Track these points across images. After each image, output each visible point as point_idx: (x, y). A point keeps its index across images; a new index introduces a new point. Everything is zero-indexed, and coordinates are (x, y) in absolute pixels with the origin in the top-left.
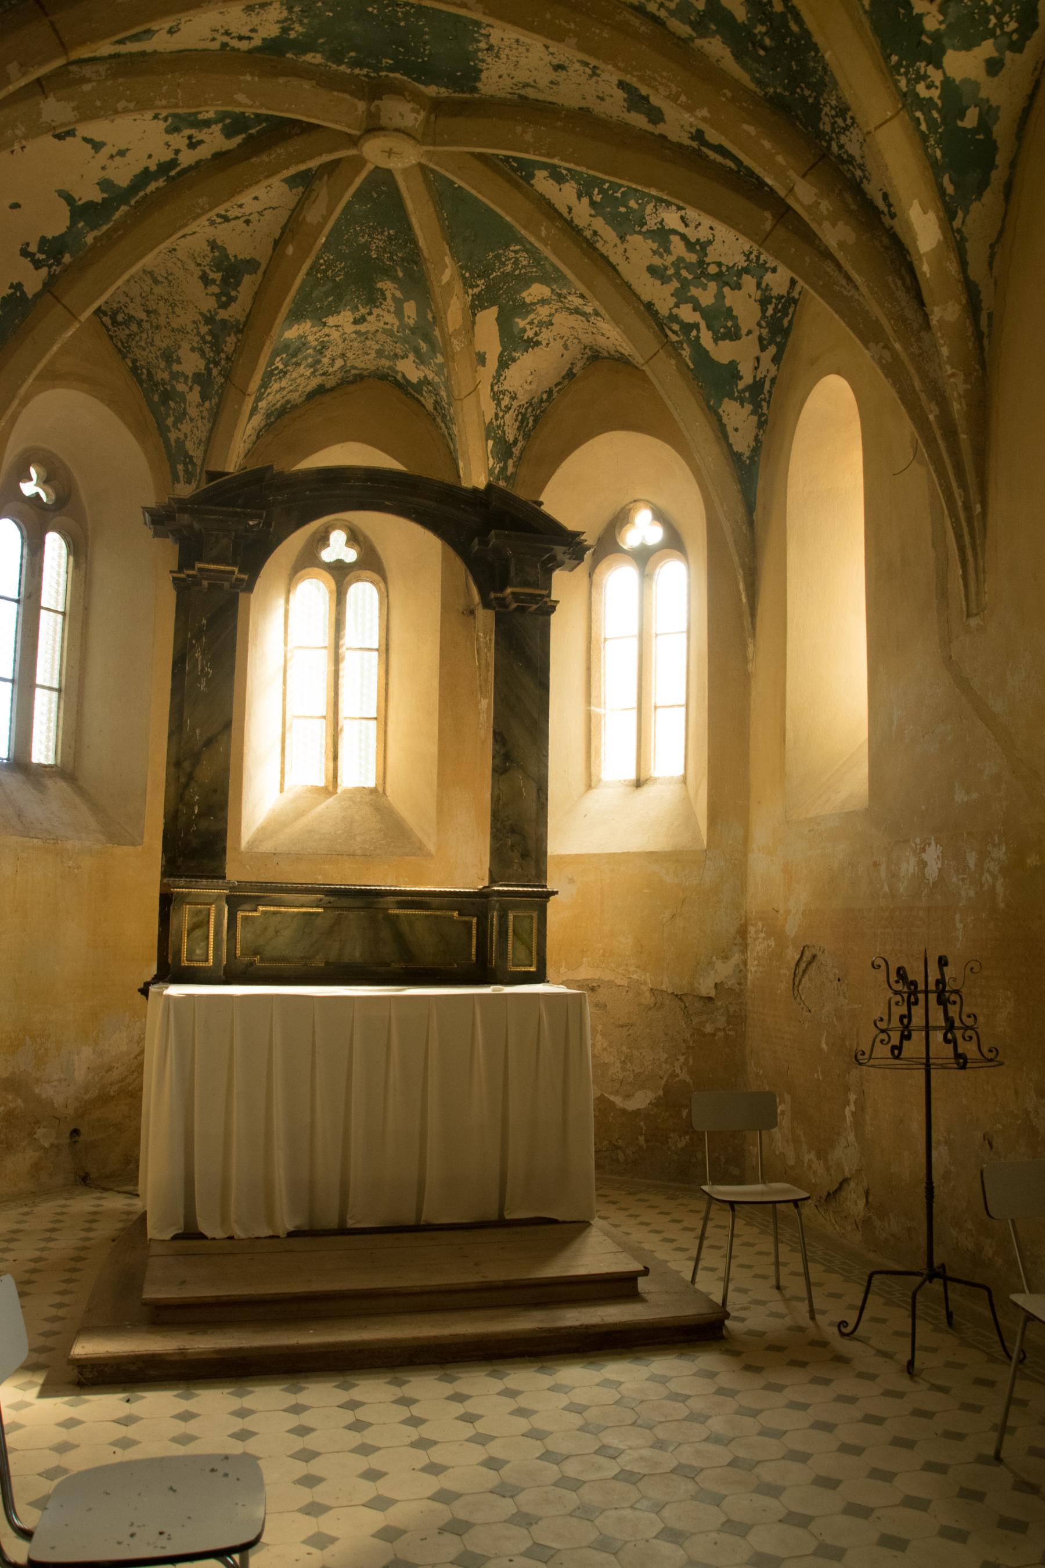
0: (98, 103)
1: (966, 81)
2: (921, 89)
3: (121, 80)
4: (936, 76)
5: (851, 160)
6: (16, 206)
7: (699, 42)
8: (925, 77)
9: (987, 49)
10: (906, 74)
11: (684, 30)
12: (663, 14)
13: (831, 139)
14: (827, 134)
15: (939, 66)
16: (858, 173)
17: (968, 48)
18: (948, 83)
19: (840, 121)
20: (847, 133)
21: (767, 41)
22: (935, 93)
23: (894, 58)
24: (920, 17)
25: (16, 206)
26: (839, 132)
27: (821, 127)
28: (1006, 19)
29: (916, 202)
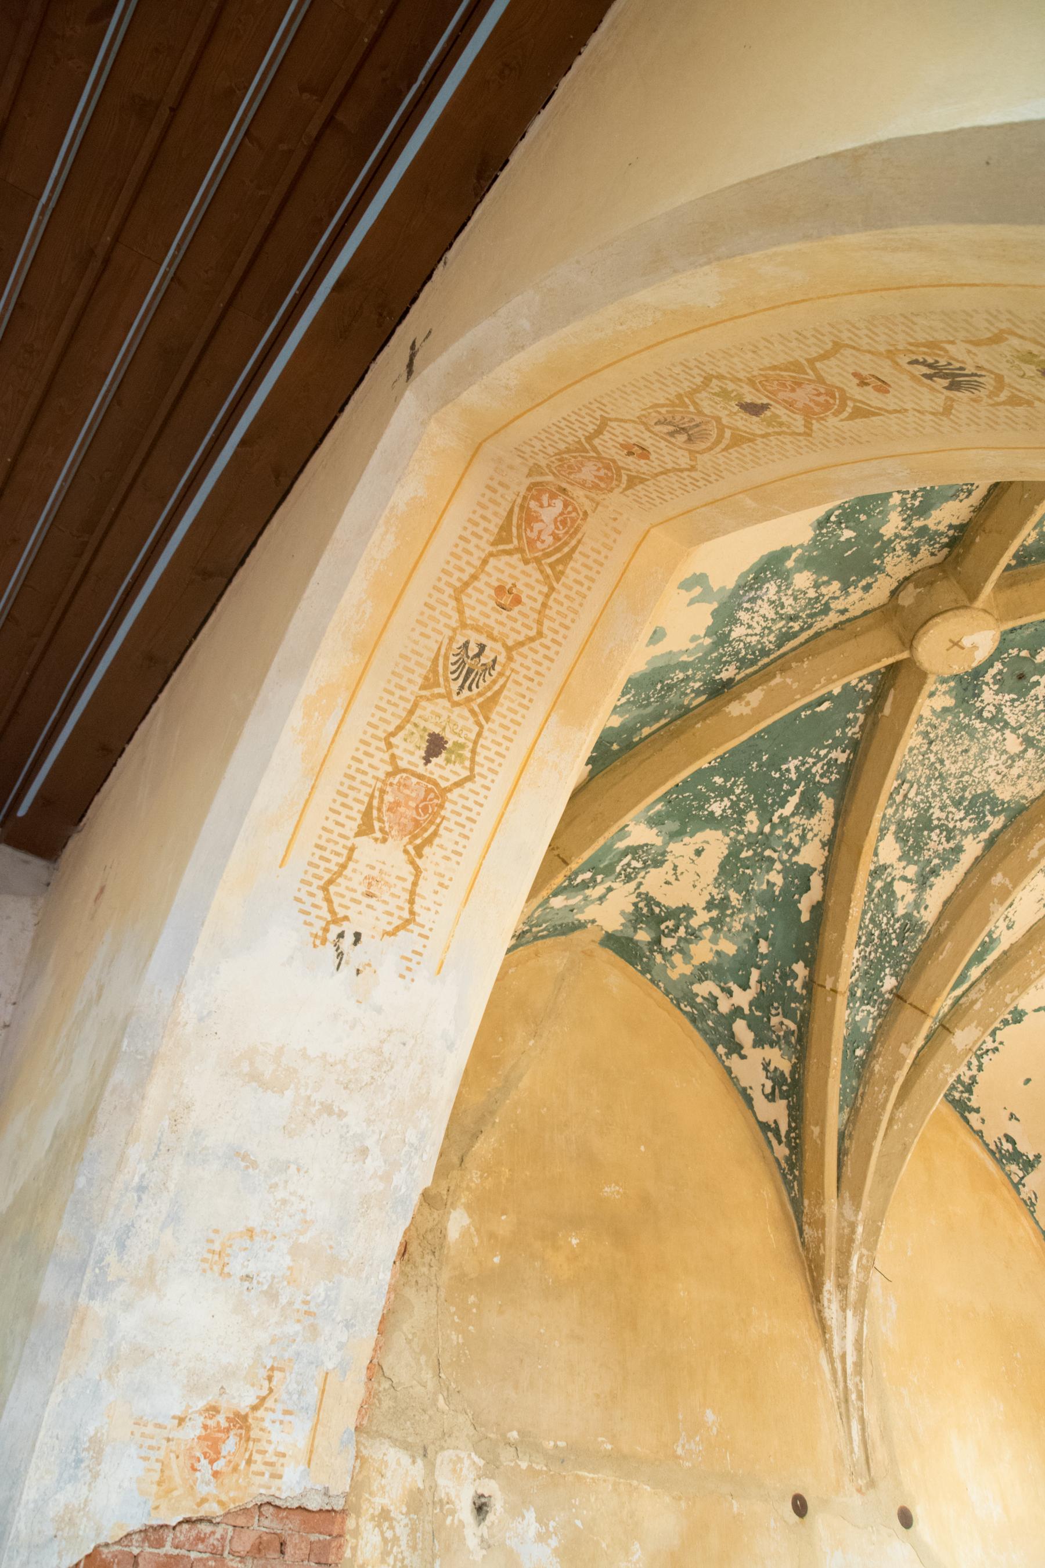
0: (992, 1010)
3: (998, 983)
6: (1028, 1081)
25: (1028, 1081)
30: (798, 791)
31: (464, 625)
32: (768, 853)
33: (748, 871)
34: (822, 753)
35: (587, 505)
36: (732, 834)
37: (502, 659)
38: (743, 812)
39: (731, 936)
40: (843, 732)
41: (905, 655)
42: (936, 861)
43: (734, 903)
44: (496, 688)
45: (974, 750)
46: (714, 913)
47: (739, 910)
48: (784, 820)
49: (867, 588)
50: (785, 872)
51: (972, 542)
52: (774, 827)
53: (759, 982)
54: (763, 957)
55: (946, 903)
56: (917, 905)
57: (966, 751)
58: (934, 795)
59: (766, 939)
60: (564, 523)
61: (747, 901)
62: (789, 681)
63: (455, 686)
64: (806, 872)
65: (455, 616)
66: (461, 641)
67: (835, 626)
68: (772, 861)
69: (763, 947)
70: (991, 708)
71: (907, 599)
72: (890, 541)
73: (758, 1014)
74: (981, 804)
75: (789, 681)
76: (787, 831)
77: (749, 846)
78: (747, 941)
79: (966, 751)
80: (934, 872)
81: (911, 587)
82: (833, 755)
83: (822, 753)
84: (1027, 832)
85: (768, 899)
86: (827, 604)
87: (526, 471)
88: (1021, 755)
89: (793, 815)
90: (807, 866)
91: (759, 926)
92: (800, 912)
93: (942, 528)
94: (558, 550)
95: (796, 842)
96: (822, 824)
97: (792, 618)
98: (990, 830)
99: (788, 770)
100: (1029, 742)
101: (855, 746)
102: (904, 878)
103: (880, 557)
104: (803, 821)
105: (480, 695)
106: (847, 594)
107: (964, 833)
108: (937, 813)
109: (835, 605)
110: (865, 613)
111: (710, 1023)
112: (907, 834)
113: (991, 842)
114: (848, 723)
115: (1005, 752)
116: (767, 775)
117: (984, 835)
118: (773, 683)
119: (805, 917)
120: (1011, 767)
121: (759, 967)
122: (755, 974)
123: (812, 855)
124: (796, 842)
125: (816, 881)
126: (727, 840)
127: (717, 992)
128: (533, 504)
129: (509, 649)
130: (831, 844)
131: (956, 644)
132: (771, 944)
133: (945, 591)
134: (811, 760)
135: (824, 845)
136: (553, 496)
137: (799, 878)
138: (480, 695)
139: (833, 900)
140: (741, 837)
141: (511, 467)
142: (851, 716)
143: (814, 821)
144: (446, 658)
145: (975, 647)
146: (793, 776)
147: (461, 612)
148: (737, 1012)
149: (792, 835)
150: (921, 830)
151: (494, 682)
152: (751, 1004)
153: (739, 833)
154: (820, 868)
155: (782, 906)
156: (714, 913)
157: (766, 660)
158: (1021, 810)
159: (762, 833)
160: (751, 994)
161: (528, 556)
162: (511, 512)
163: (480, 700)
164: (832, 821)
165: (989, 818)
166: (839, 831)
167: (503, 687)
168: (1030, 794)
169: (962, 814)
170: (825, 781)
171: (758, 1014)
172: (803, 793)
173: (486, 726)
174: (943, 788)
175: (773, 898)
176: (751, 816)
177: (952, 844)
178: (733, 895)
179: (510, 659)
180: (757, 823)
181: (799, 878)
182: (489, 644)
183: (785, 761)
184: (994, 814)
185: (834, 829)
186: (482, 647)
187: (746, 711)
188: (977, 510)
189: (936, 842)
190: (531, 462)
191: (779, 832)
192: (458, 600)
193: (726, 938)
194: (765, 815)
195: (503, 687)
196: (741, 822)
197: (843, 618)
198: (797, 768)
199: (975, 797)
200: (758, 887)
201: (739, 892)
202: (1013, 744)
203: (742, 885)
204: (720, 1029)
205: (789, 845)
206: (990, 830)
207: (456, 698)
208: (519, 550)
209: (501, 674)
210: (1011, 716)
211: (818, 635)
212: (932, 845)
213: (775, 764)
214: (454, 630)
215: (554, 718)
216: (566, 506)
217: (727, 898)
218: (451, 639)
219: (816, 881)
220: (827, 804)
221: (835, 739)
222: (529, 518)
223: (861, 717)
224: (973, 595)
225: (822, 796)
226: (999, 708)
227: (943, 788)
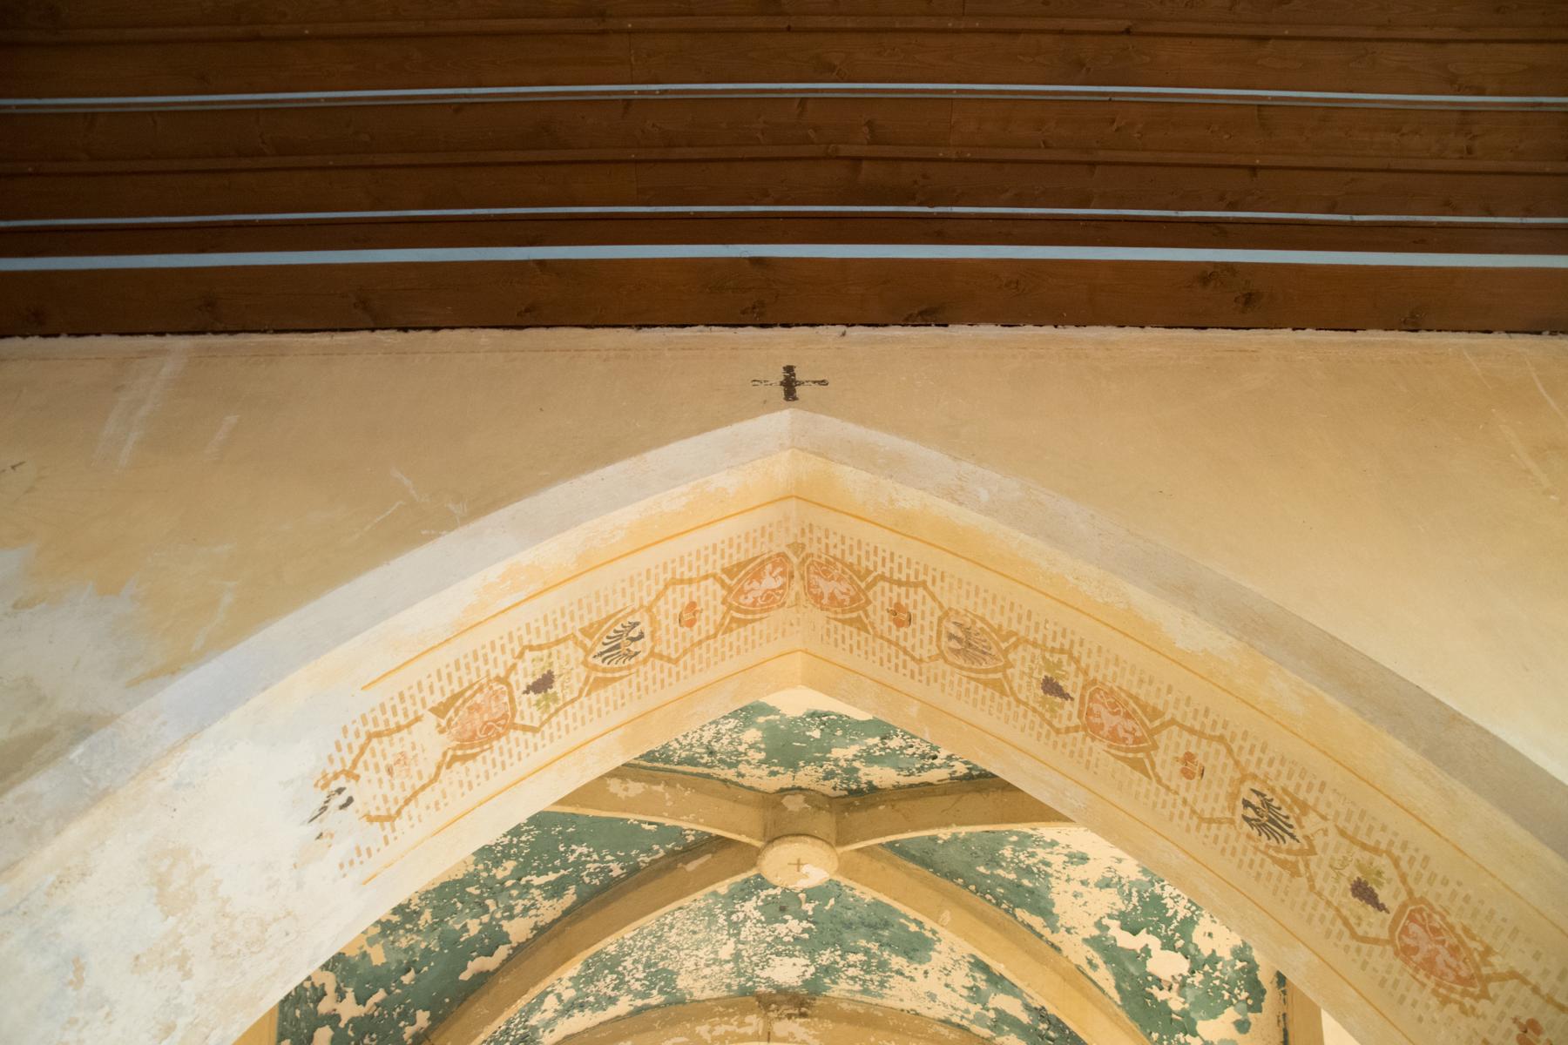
7: (999, 1040)
11: (986, 1033)
12: (965, 1023)
15: (1195, 1034)
17: (1215, 1016)
21: (1052, 1034)
23: (1155, 1036)
28: (1236, 991)
30: (562, 872)
31: (649, 609)
32: (489, 902)
33: (459, 905)
34: (609, 858)
35: (791, 599)
36: (481, 866)
37: (641, 657)
38: (508, 857)
39: (390, 949)
40: (637, 855)
41: (758, 844)
42: (591, 999)
43: (421, 922)
44: (617, 675)
45: (700, 936)
46: (396, 919)
47: (419, 931)
48: (528, 886)
49: (773, 774)
50: (486, 927)
51: (874, 805)
52: (513, 887)
53: (377, 1005)
54: (401, 985)
55: (567, 1038)
56: (549, 1024)
57: (694, 933)
58: (641, 948)
59: (417, 972)
60: (768, 597)
61: (432, 928)
62: (667, 796)
63: (600, 648)
64: (504, 938)
65: (653, 597)
66: (636, 618)
67: (725, 781)
68: (486, 910)
69: (407, 979)
70: (741, 915)
71: (794, 804)
72: (828, 760)
73: (351, 1033)
74: (661, 977)
75: (667, 796)
76: (520, 896)
77: (481, 886)
78: (400, 962)
79: (694, 933)
80: (582, 1007)
81: (800, 798)
82: (612, 865)
83: (609, 858)
84: (674, 1023)
85: (450, 940)
86: (739, 762)
87: (791, 540)
88: (721, 963)
89: (539, 887)
90: (507, 935)
91: (422, 956)
92: (465, 968)
93: (864, 779)
94: (746, 612)
95: (518, 910)
96: (549, 910)
97: (712, 753)
98: (647, 1001)
99: (573, 851)
100: (737, 956)
101: (634, 870)
102: (559, 996)
103: (808, 763)
104: (540, 898)
105: (604, 671)
106: (758, 767)
107: (629, 991)
108: (628, 963)
109: (743, 768)
110: (751, 788)
111: (298, 1013)
112: (594, 963)
113: (639, 1011)
114: (649, 851)
115: (716, 952)
116: (557, 842)
117: (639, 1003)
118: (655, 788)
119: (465, 976)
120: (708, 966)
121: (389, 992)
122: (380, 995)
123: (518, 929)
124: (518, 910)
125: (502, 952)
126: (471, 869)
127: (330, 989)
128: (769, 567)
129: (652, 654)
130: (540, 931)
131: (799, 864)
132: (417, 980)
133: (825, 822)
134: (595, 857)
135: (535, 927)
136: (782, 574)
137: (492, 939)
138: (604, 671)
139: (507, 979)
140: (485, 874)
141: (787, 530)
142: (656, 847)
143: (547, 903)
144: (616, 623)
145: (806, 876)
146: (571, 859)
147: (658, 598)
148: (333, 1019)
149: (521, 902)
150: (606, 967)
151: (621, 669)
152: (352, 1020)
153: (487, 869)
154: (514, 944)
155: (459, 951)
156: (396, 919)
157: (661, 765)
158: (682, 1002)
159: (502, 883)
160: (360, 1011)
161: (729, 599)
162: (755, 559)
163: (600, 675)
164: (559, 914)
165: (655, 992)
166: (557, 926)
167: (621, 678)
168: (697, 995)
169: (642, 976)
170: (587, 880)
171: (351, 1033)
172: (563, 876)
173: (583, 699)
174: (652, 948)
175: (456, 942)
176: (510, 865)
177: (612, 994)
178: (427, 916)
179: (645, 661)
180: (507, 873)
181: (492, 939)
182: (647, 638)
183: (580, 843)
184: (661, 991)
185: (554, 922)
186: (641, 636)
187: (622, 794)
188: (898, 788)
189: (606, 984)
190: (805, 540)
191: (515, 893)
192: (666, 587)
193: (384, 946)
194: (518, 875)
195: (621, 678)
196: (497, 863)
197: (735, 779)
198: (581, 854)
199: (664, 970)
200: (453, 924)
201: (434, 916)
202: (726, 952)
203: (441, 912)
204: (303, 1024)
205: (510, 908)
206: (647, 1001)
207: (590, 659)
208: (730, 590)
209: (629, 667)
210: (746, 932)
211: (708, 776)
212: (601, 984)
213: (569, 840)
214: (642, 606)
215: (620, 731)
216: (781, 587)
217: (418, 914)
218: (633, 612)
219: (502, 952)
220: (570, 897)
221: (628, 855)
222: (757, 575)
223: (662, 853)
224: (841, 841)
225: (572, 889)
226: (746, 918)
227: (652, 948)
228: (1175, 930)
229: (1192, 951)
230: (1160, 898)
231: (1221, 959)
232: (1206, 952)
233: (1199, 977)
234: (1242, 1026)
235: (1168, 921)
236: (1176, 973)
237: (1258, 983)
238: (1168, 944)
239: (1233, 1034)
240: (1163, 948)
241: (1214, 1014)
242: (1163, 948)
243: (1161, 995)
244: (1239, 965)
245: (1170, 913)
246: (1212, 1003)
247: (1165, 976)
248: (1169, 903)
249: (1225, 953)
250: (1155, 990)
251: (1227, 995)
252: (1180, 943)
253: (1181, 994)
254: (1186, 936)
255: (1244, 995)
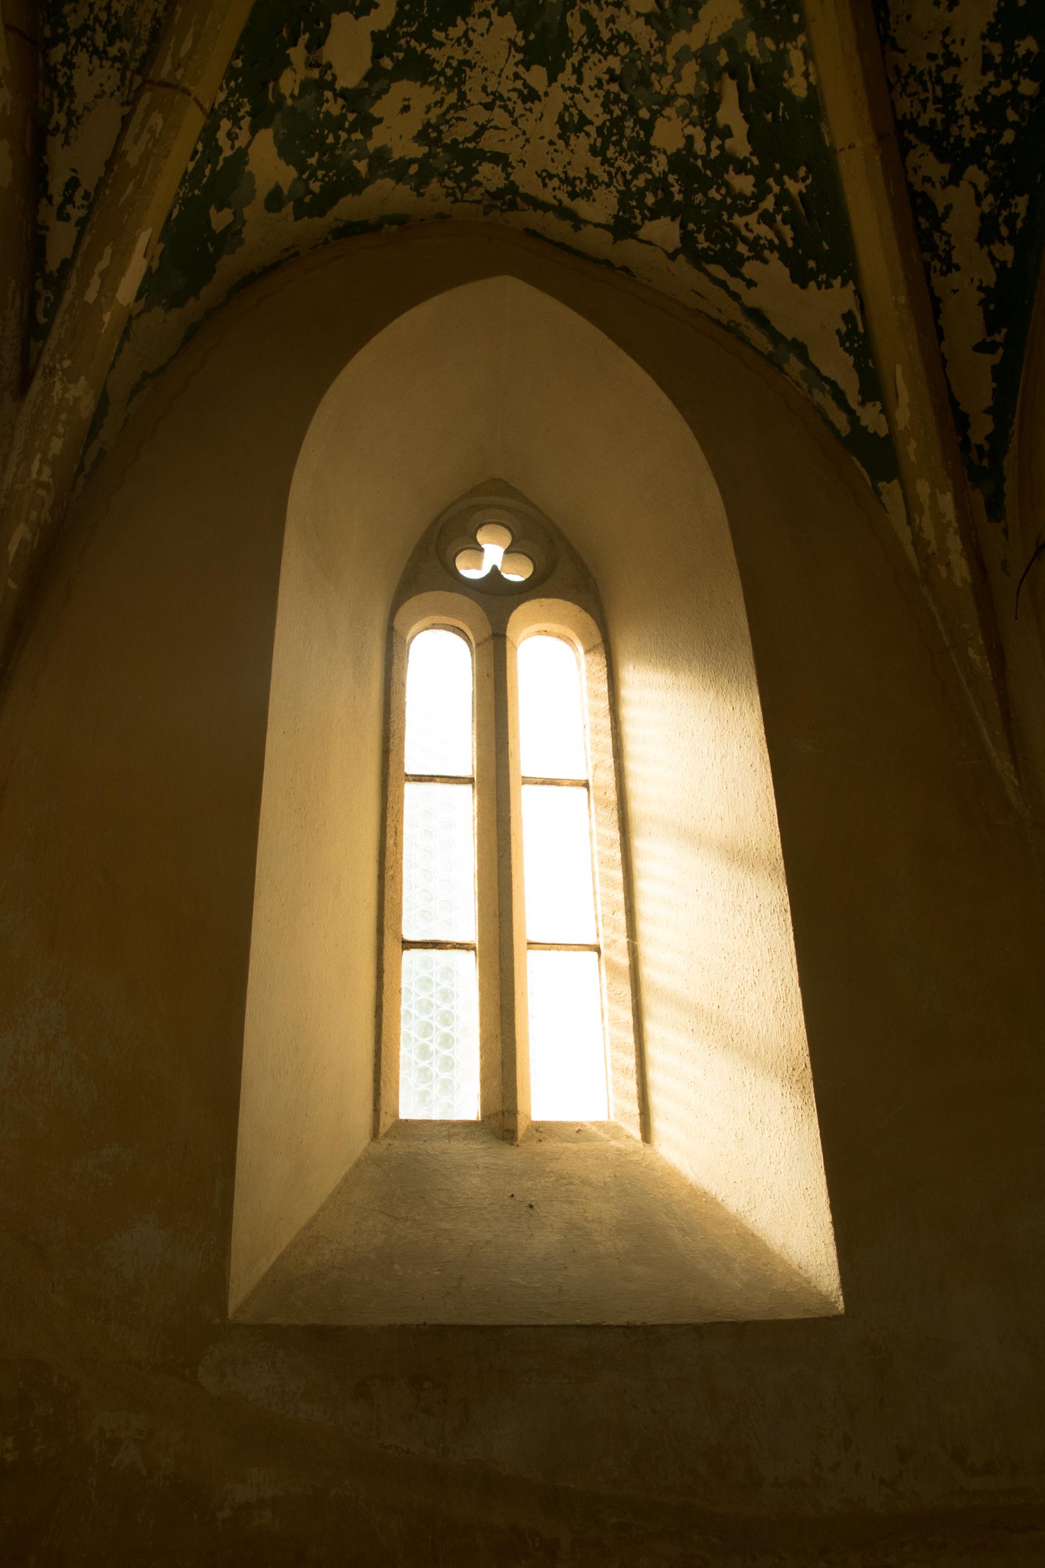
1: (251, 177)
2: (226, 125)
4: (244, 137)
5: (67, 93)
8: (236, 122)
9: (286, 175)
10: (231, 93)
13: (64, 38)
14: (66, 26)
15: (254, 130)
16: (60, 118)
17: (281, 154)
18: (241, 156)
19: (100, 37)
20: (95, 58)
22: (228, 152)
23: (239, 63)
24: (287, 63)
26: (84, 45)
27: (67, 9)
29: (150, 230)
228: (410, 51)
229: (377, 87)
230: (466, 14)
231: (368, 135)
232: (377, 110)
233: (334, 107)
234: (275, 200)
235: (424, 35)
236: (337, 70)
237: (333, 202)
238: (382, 43)
239: (263, 188)
240: (377, 37)
241: (285, 151)
242: (377, 37)
243: (297, 54)
244: (362, 166)
245: (438, 35)
246: (300, 140)
247: (332, 51)
248: (455, 32)
249: (379, 138)
250: (305, 38)
251: (313, 161)
252: (387, 63)
253: (306, 86)
254: (401, 71)
255: (315, 186)
